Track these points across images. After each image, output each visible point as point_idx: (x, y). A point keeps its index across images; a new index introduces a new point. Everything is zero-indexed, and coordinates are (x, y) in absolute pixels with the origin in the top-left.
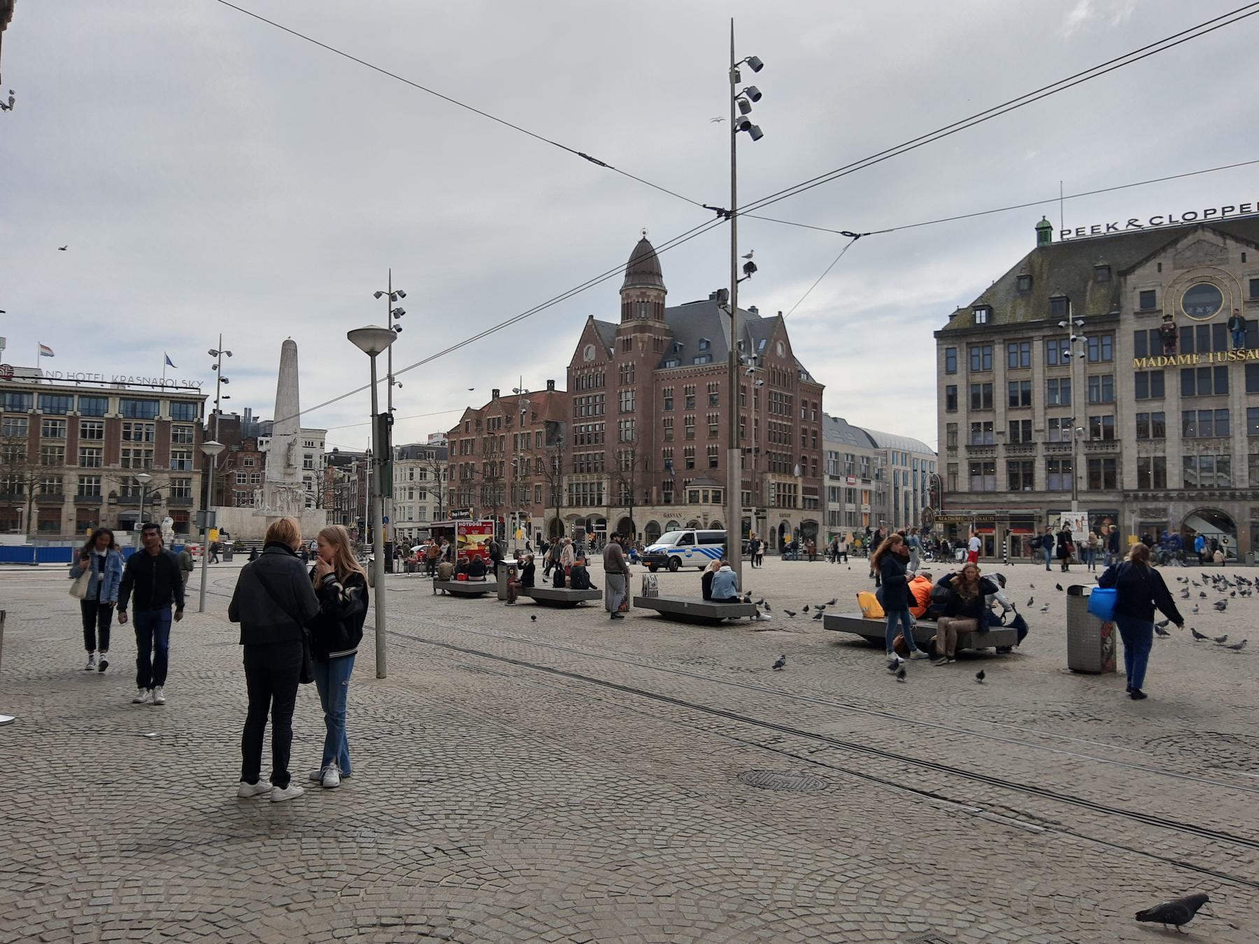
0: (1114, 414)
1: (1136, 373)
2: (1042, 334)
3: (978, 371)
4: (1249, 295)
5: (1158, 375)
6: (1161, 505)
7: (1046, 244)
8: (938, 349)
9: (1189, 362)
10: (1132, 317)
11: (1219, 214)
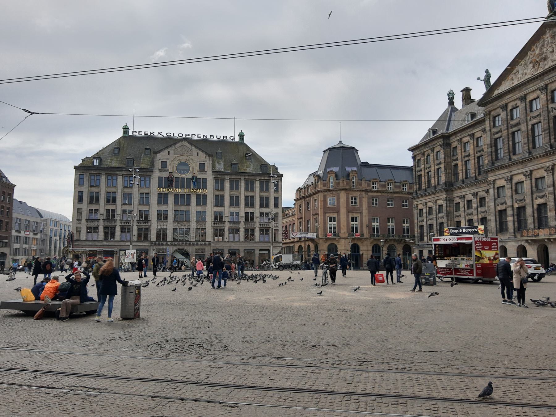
2: (122, 173)
3: (93, 186)
4: (198, 169)
5: (166, 195)
6: (164, 247)
7: (126, 135)
8: (75, 174)
10: (158, 171)
11: (190, 136)
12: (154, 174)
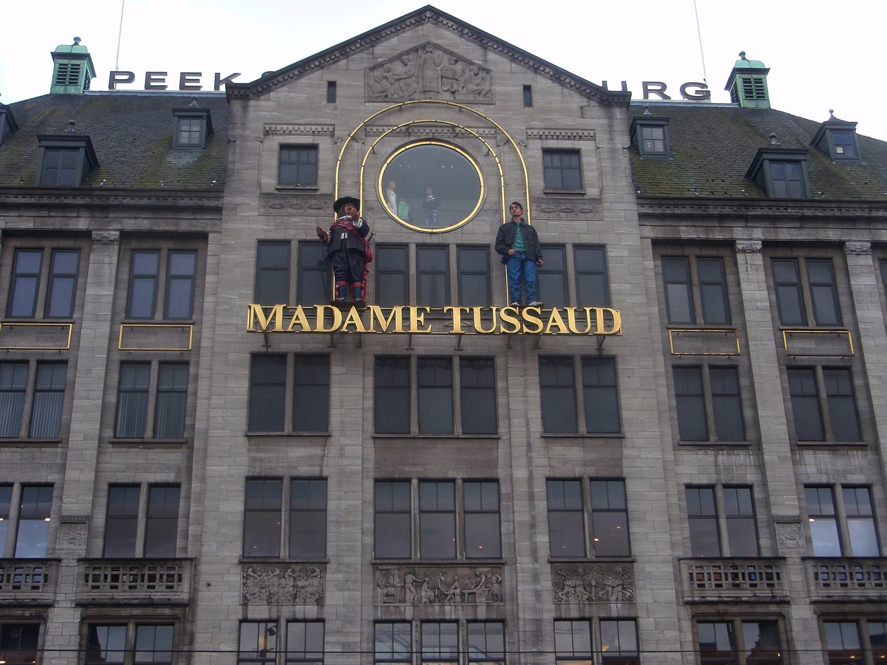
0: (183, 480)
1: (255, 357)
4: (540, 183)
7: (72, 90)
9: (399, 327)
10: (254, 202)
12: (229, 224)
